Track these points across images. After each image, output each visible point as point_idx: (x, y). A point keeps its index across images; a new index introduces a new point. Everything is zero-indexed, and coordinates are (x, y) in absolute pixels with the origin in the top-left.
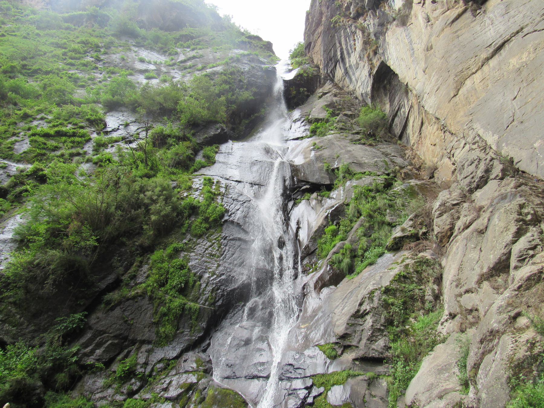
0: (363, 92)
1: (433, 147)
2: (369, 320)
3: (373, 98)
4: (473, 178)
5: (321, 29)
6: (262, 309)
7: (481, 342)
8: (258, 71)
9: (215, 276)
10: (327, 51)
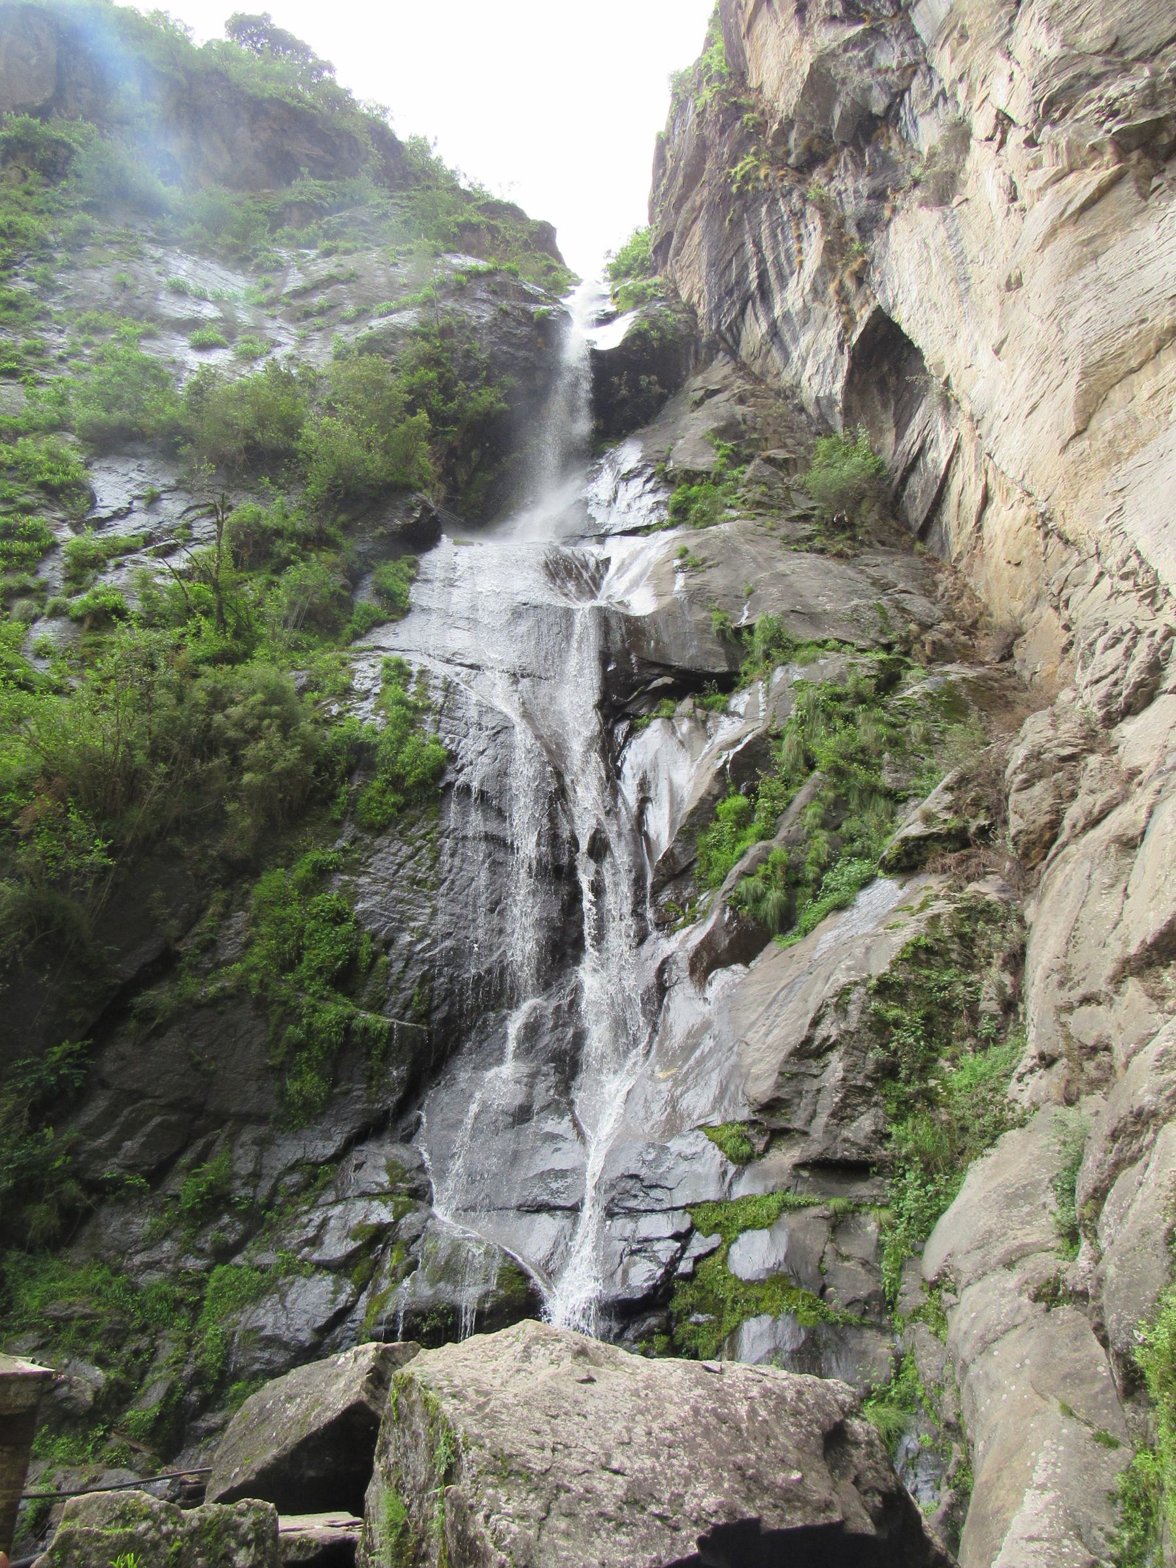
0: (821, 394)
1: (1013, 570)
2: (836, 1066)
3: (847, 411)
4: (1115, 684)
5: (701, 195)
6: (555, 1027)
7: (1114, 1136)
8: (520, 323)
9: (428, 941)
10: (718, 266)
